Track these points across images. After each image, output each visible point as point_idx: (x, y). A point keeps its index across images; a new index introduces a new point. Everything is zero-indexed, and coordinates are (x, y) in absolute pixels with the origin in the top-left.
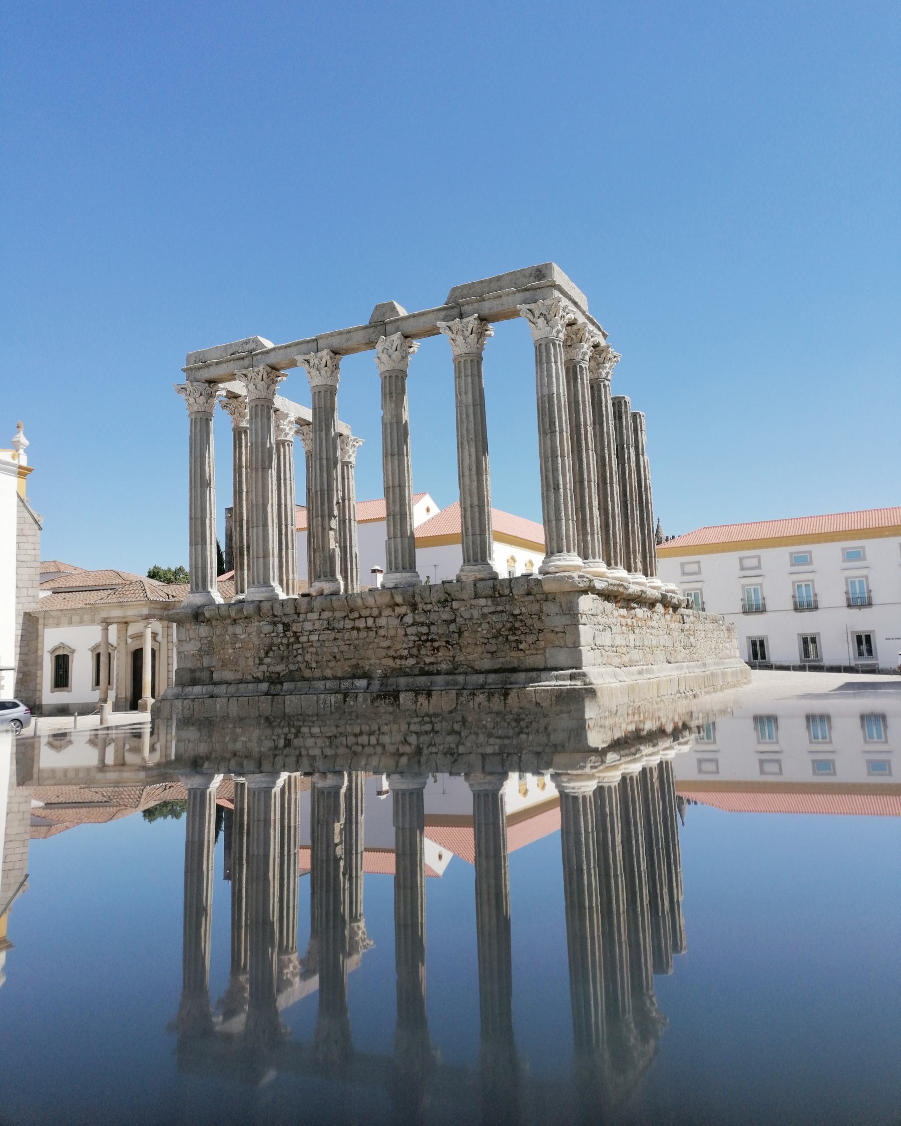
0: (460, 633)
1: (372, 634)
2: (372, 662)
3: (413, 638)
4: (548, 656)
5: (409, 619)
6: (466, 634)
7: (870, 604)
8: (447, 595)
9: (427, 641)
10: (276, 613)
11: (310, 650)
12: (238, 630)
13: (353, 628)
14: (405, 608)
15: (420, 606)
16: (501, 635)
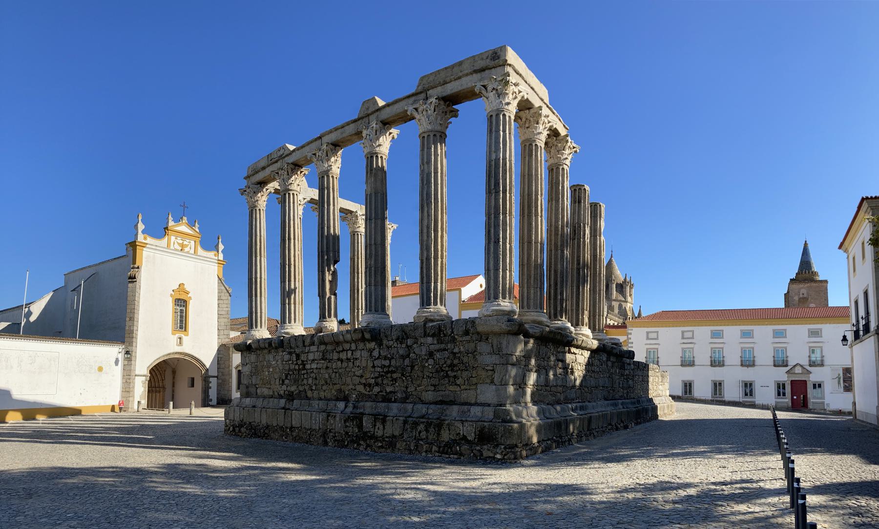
0: (412, 367)
1: (351, 364)
2: (351, 387)
3: (379, 369)
4: (479, 391)
5: (376, 353)
6: (416, 368)
7: (754, 365)
8: (404, 332)
9: (388, 372)
10: (293, 346)
11: (312, 375)
12: (271, 357)
13: (338, 359)
14: (374, 343)
15: (385, 342)
16: (443, 371)
